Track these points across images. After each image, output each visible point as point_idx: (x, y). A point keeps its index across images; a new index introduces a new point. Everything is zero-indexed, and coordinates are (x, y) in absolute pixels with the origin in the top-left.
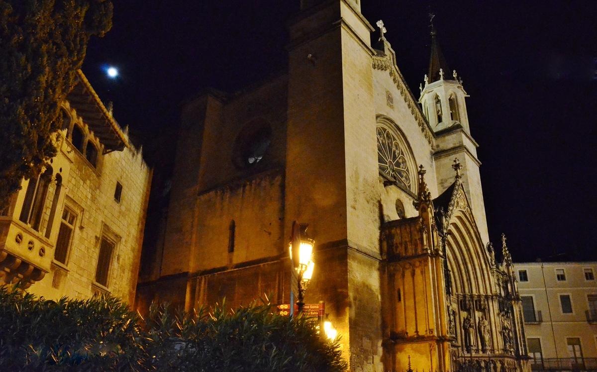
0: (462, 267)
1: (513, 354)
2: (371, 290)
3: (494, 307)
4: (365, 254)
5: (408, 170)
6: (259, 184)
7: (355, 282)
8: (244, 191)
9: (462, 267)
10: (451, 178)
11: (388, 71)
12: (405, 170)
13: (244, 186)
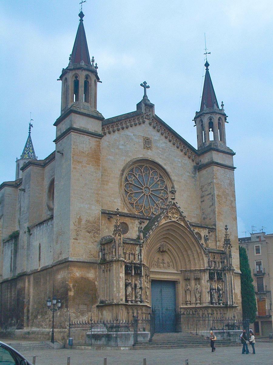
0: (184, 253)
1: (221, 304)
3: (206, 276)
5: (166, 188)
6: (48, 224)
8: (43, 226)
9: (184, 253)
10: (206, 185)
11: (147, 122)
12: (163, 188)
13: (43, 224)
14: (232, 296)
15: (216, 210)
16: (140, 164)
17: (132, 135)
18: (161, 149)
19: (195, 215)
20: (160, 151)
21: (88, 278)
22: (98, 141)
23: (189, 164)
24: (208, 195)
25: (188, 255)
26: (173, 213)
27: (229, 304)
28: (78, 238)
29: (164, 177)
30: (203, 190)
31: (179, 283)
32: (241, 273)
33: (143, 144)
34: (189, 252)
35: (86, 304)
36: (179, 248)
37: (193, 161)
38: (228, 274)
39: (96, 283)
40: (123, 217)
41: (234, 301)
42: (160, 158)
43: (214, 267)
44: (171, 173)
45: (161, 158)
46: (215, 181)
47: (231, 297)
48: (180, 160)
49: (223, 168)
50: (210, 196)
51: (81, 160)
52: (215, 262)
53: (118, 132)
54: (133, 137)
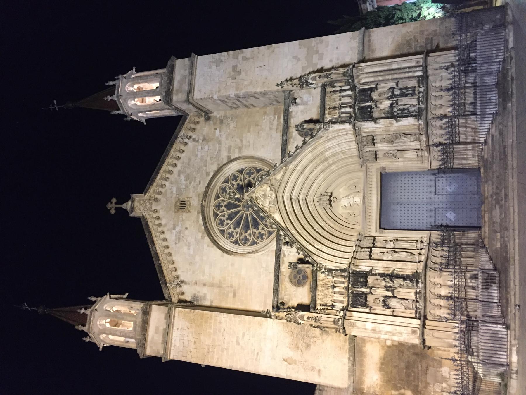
0: (330, 161)
1: (422, 90)
2: (384, 359)
3: (368, 127)
4: (353, 365)
5: (241, 171)
7: (381, 383)
9: (330, 161)
14: (404, 68)
15: (259, 90)
16: (212, 218)
17: (174, 231)
18: (188, 182)
19: (276, 116)
20: (190, 183)
21: (381, 359)
22: (178, 315)
23: (205, 128)
24: (240, 101)
25: (334, 155)
26: (265, 196)
27: (420, 74)
28: (317, 368)
29: (227, 175)
30: (235, 106)
31: (383, 168)
32: (363, 28)
33: (184, 214)
34: (328, 154)
35: (427, 369)
36: (323, 171)
37: (198, 122)
38: (361, 79)
39: (389, 343)
40: (281, 278)
41: (414, 64)
42: (200, 184)
43: (351, 107)
44: (218, 164)
45: (200, 181)
46: (215, 97)
47: (407, 70)
48: (200, 148)
49: (196, 79)
50: (240, 99)
51: (206, 347)
52: (340, 107)
53: (173, 254)
54: (177, 229)
